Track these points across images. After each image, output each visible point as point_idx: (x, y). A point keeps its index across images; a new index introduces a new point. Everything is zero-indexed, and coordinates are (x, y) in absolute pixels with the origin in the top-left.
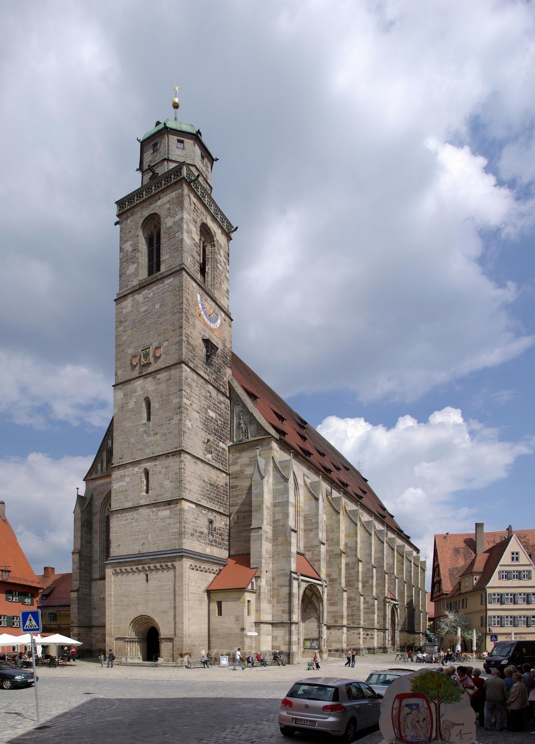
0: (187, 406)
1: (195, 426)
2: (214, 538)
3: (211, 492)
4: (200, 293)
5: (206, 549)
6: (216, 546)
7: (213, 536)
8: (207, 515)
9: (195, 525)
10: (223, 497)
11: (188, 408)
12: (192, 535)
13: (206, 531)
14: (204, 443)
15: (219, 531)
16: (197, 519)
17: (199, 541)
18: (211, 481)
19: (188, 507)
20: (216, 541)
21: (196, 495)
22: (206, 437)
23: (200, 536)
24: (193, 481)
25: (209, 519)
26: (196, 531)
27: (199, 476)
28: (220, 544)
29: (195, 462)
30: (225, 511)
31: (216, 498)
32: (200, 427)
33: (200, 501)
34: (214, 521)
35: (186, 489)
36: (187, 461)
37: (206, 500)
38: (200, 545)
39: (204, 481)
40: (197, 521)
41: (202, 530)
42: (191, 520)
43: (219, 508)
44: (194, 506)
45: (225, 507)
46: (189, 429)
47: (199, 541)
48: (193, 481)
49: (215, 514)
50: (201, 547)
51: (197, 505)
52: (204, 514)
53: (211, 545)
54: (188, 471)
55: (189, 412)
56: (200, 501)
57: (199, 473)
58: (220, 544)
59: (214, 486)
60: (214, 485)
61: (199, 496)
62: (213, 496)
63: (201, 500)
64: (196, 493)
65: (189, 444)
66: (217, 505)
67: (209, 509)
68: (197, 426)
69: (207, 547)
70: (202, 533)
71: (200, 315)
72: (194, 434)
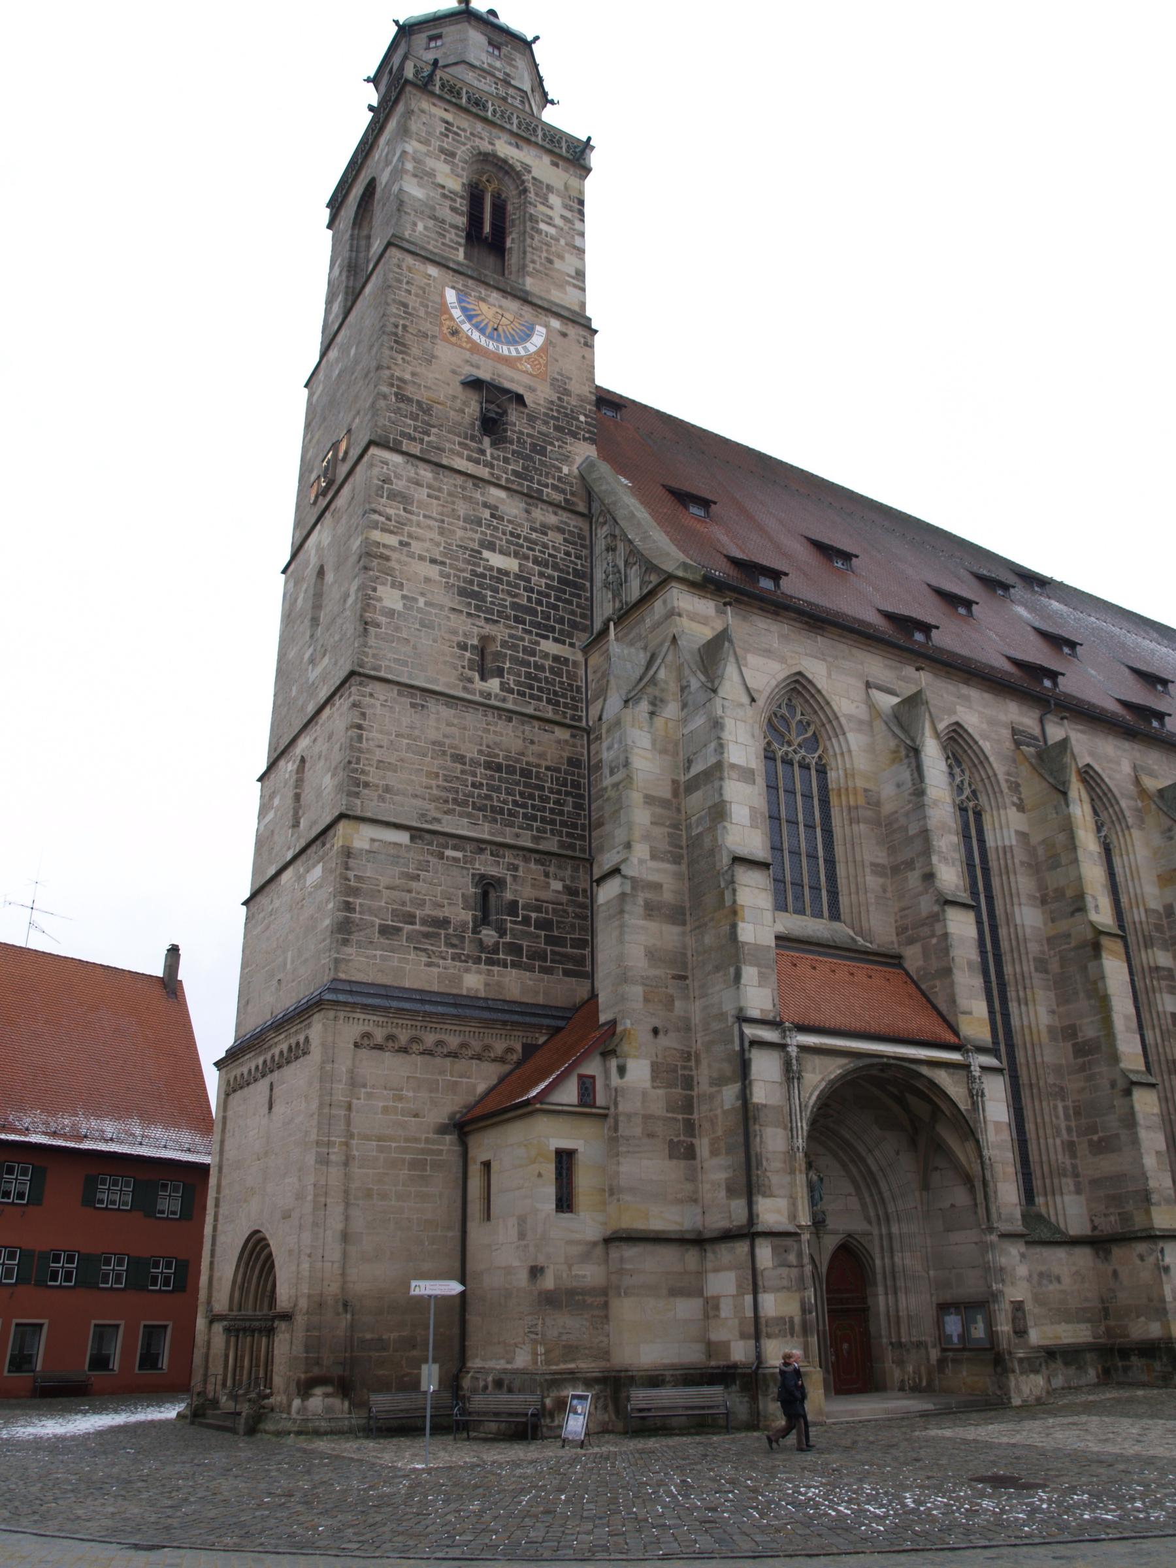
0: (382, 550)
1: (421, 603)
2: (508, 939)
3: (498, 790)
4: (460, 286)
5: (460, 979)
6: (514, 965)
7: (502, 932)
8: (473, 861)
9: (407, 897)
10: (557, 802)
11: (387, 552)
12: (385, 931)
13: (464, 915)
14: (463, 647)
15: (534, 915)
16: (416, 878)
17: (425, 950)
18: (497, 756)
19: (373, 840)
20: (515, 949)
21: (418, 802)
22: (475, 630)
23: (427, 935)
24: (402, 760)
25: (483, 877)
26: (410, 919)
27: (434, 743)
28: (540, 956)
29: (413, 705)
30: (572, 847)
31: (524, 806)
32: (442, 607)
33: (438, 821)
34: (509, 879)
35: (367, 785)
36: (378, 704)
37: (469, 815)
38: (429, 965)
39: (459, 758)
40: (414, 885)
41: (439, 914)
42: (384, 881)
43: (536, 839)
44: (403, 838)
45: (569, 835)
46: (391, 613)
47: (425, 950)
48: (402, 760)
49: (509, 857)
50: (435, 970)
51: (416, 833)
52: (456, 860)
53: (490, 962)
54: (381, 732)
55: (393, 564)
56: (438, 821)
57: (433, 735)
58: (540, 956)
59: (511, 770)
60: (508, 766)
61: (427, 805)
62: (505, 802)
63: (439, 816)
64: (416, 796)
65: (390, 655)
66: (530, 828)
67: (480, 845)
68: (426, 604)
69: (467, 970)
70: (444, 923)
71: (455, 332)
72: (417, 626)
